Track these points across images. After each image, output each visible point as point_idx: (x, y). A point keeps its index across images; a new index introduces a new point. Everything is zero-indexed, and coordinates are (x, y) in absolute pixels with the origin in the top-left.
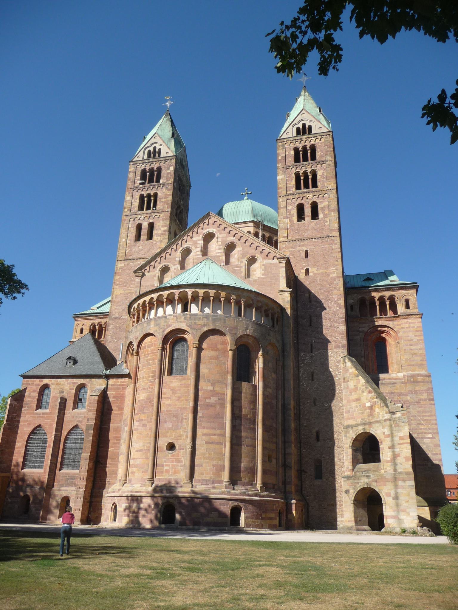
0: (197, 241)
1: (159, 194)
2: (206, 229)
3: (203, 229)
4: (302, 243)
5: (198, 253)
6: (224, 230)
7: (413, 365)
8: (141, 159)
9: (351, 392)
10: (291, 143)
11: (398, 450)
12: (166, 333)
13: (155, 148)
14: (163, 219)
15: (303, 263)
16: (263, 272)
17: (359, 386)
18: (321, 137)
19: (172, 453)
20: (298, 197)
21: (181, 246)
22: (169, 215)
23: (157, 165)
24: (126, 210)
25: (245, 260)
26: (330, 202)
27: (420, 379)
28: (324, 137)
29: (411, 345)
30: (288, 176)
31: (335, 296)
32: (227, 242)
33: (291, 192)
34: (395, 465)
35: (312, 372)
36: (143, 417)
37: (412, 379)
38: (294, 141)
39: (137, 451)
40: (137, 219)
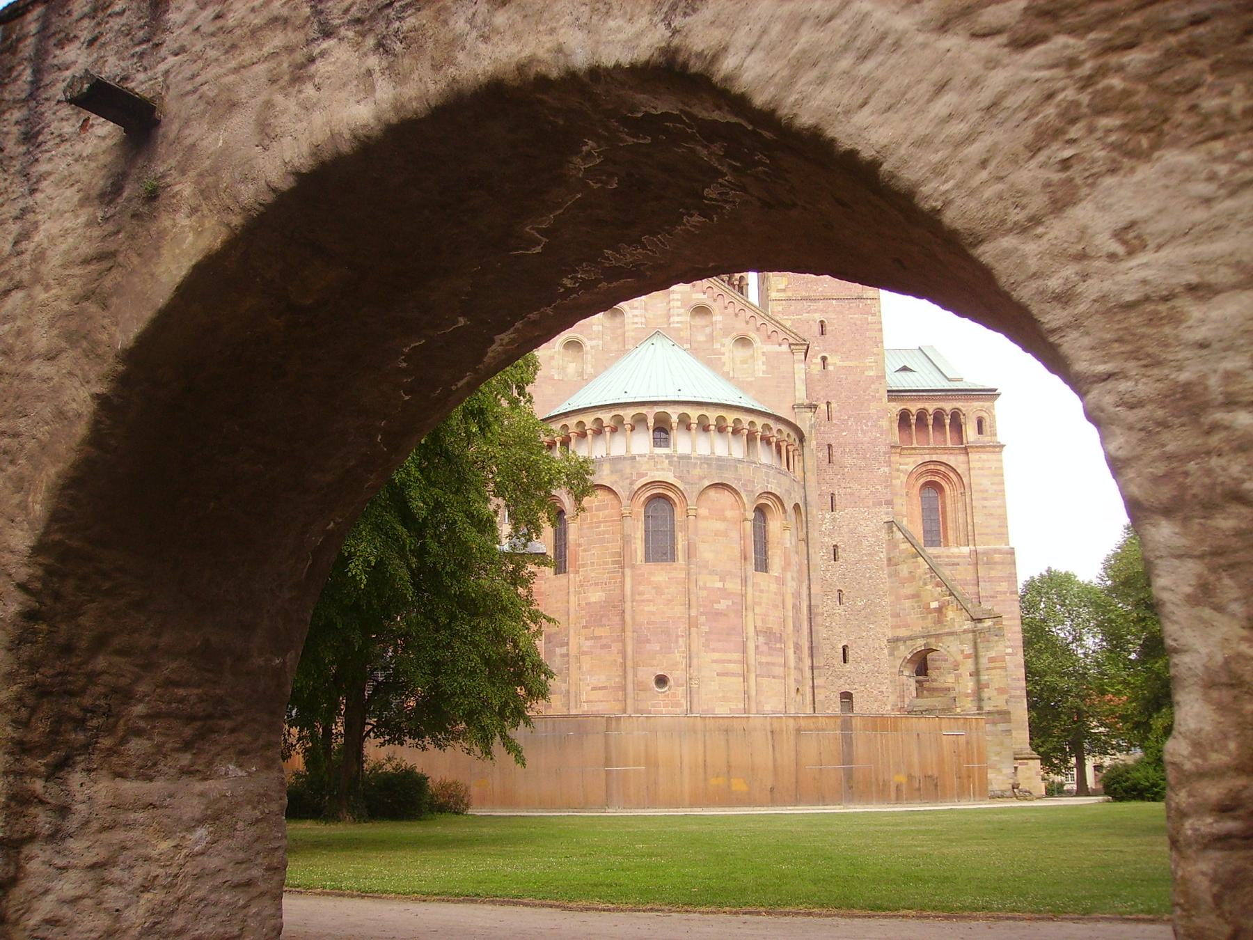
4: (814, 305)
5: (636, 320)
7: (987, 534)
9: (903, 583)
11: (986, 677)
12: (636, 487)
15: (816, 344)
16: (764, 368)
17: (919, 572)
19: (663, 692)
25: (729, 342)
27: (997, 557)
29: (985, 499)
31: (873, 411)
32: (693, 303)
34: (980, 700)
35: (834, 546)
36: (599, 632)
37: (985, 558)
39: (593, 689)
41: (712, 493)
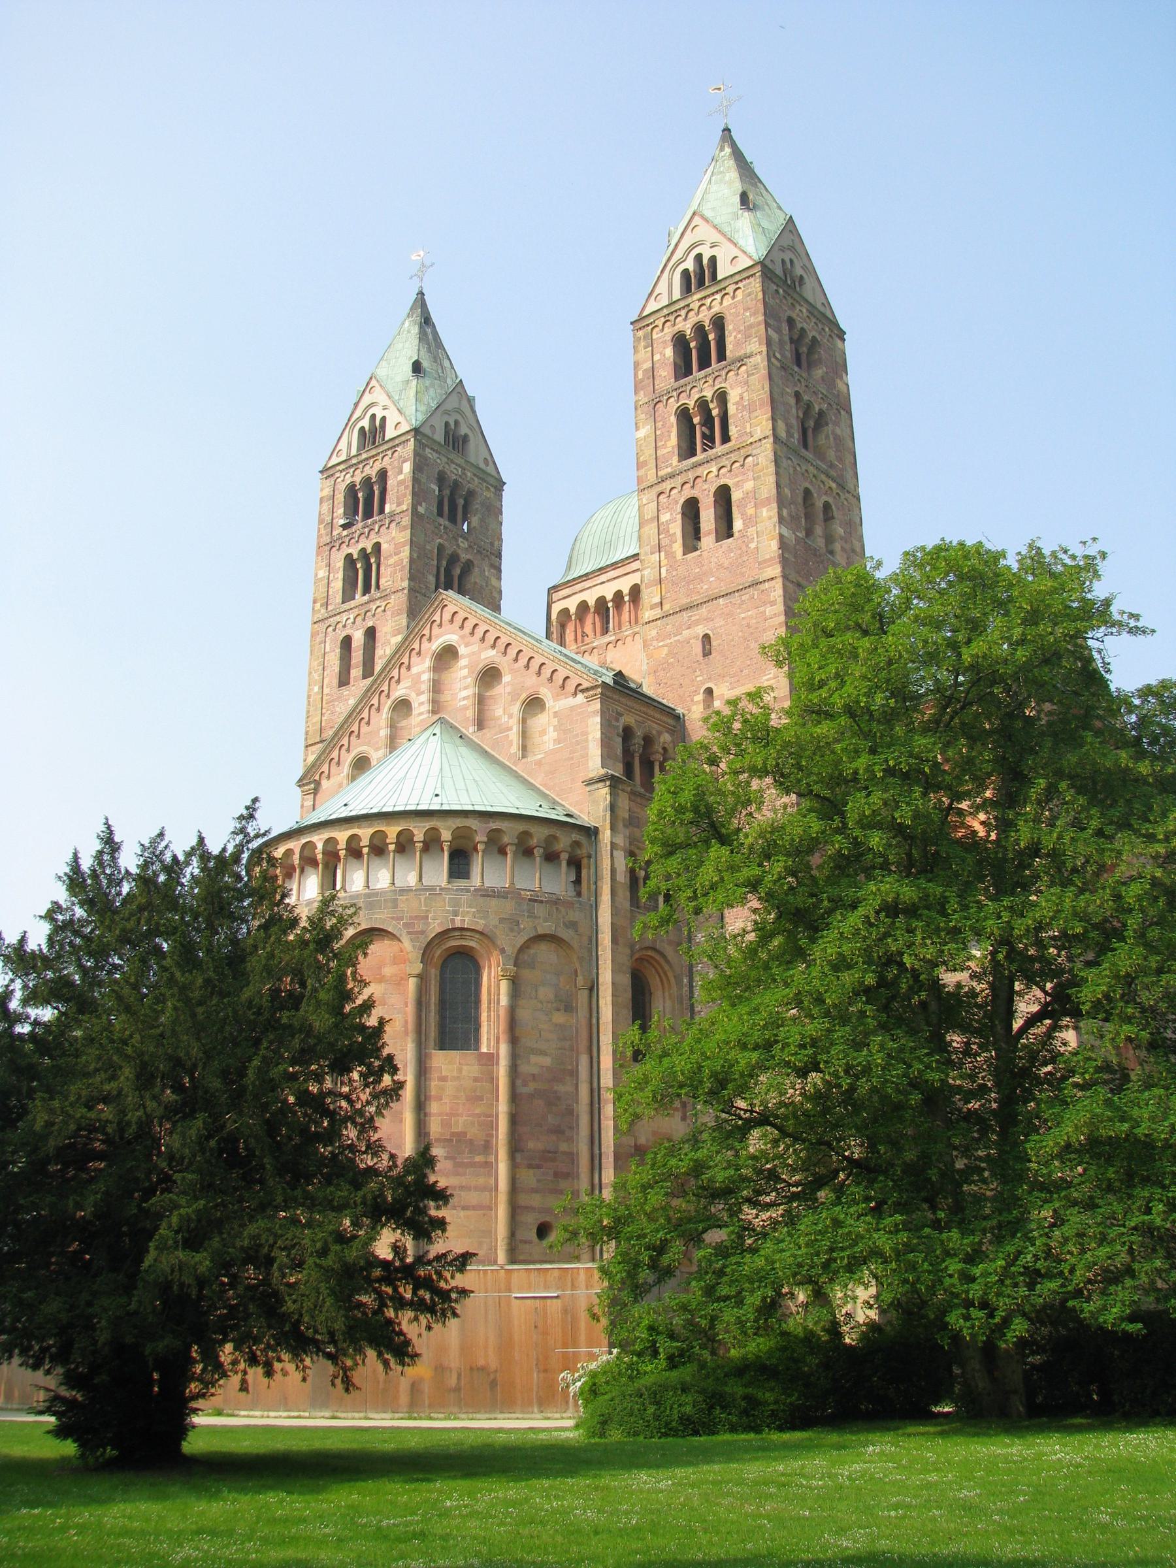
0: (419, 674)
1: (384, 547)
2: (438, 637)
3: (430, 640)
4: (696, 615)
6: (472, 633)
8: (344, 457)
10: (664, 323)
13: (373, 416)
14: (393, 615)
18: (734, 287)
20: (684, 480)
21: (388, 696)
22: (405, 598)
23: (378, 466)
26: (759, 477)
28: (740, 285)
30: (659, 425)
32: (481, 666)
33: (669, 470)
38: (672, 318)
40: (340, 625)
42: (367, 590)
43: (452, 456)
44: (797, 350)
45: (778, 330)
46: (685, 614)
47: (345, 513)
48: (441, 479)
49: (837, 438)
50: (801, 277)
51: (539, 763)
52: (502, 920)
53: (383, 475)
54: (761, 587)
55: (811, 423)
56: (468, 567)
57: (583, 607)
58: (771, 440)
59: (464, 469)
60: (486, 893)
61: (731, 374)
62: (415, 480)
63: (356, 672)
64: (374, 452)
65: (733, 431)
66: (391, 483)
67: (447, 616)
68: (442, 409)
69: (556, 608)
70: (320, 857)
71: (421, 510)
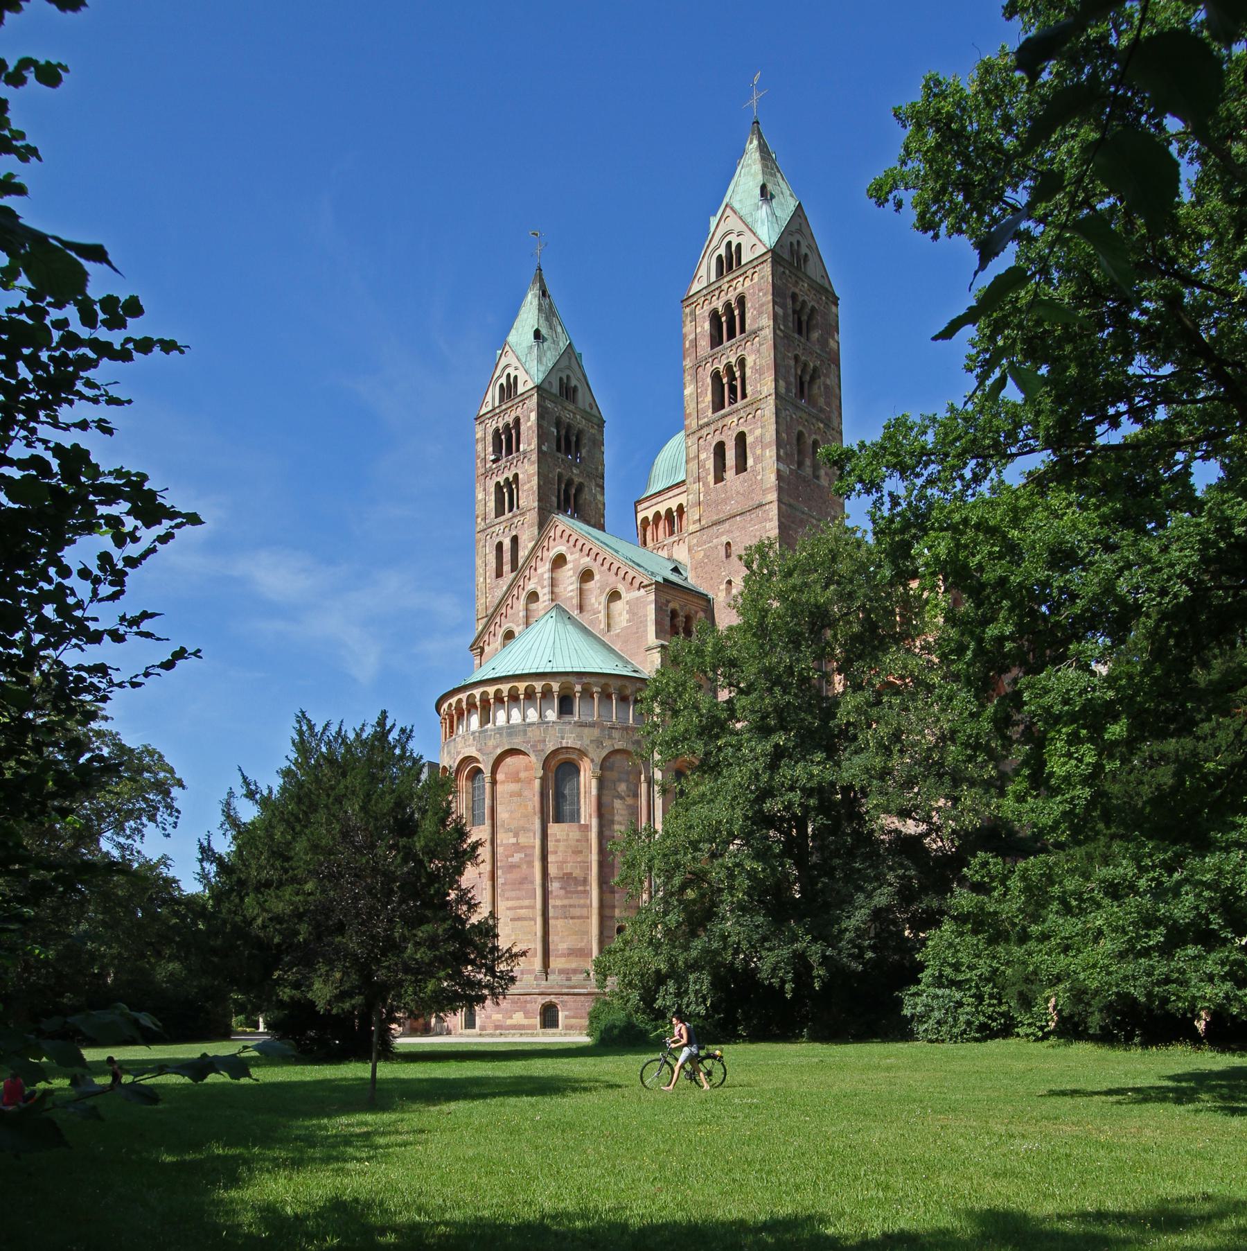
0: (542, 574)
1: (521, 476)
2: (553, 548)
3: (548, 549)
4: (722, 528)
6: (575, 546)
8: (490, 408)
13: (509, 375)
21: (523, 589)
23: (513, 415)
24: (479, 520)
41: (509, 760)
42: (511, 510)
43: (566, 404)
44: (799, 319)
45: (783, 306)
46: (715, 528)
47: (494, 451)
48: (558, 423)
49: (826, 387)
50: (806, 255)
51: (618, 635)
52: (592, 741)
53: (517, 421)
54: (764, 508)
55: (807, 378)
56: (580, 488)
57: (657, 516)
58: (774, 397)
59: (574, 413)
60: (582, 725)
61: (749, 343)
62: (539, 426)
63: (507, 568)
64: (510, 404)
65: (749, 390)
66: (522, 428)
67: (558, 533)
68: (557, 367)
69: (640, 516)
70: (478, 703)
71: (544, 448)
